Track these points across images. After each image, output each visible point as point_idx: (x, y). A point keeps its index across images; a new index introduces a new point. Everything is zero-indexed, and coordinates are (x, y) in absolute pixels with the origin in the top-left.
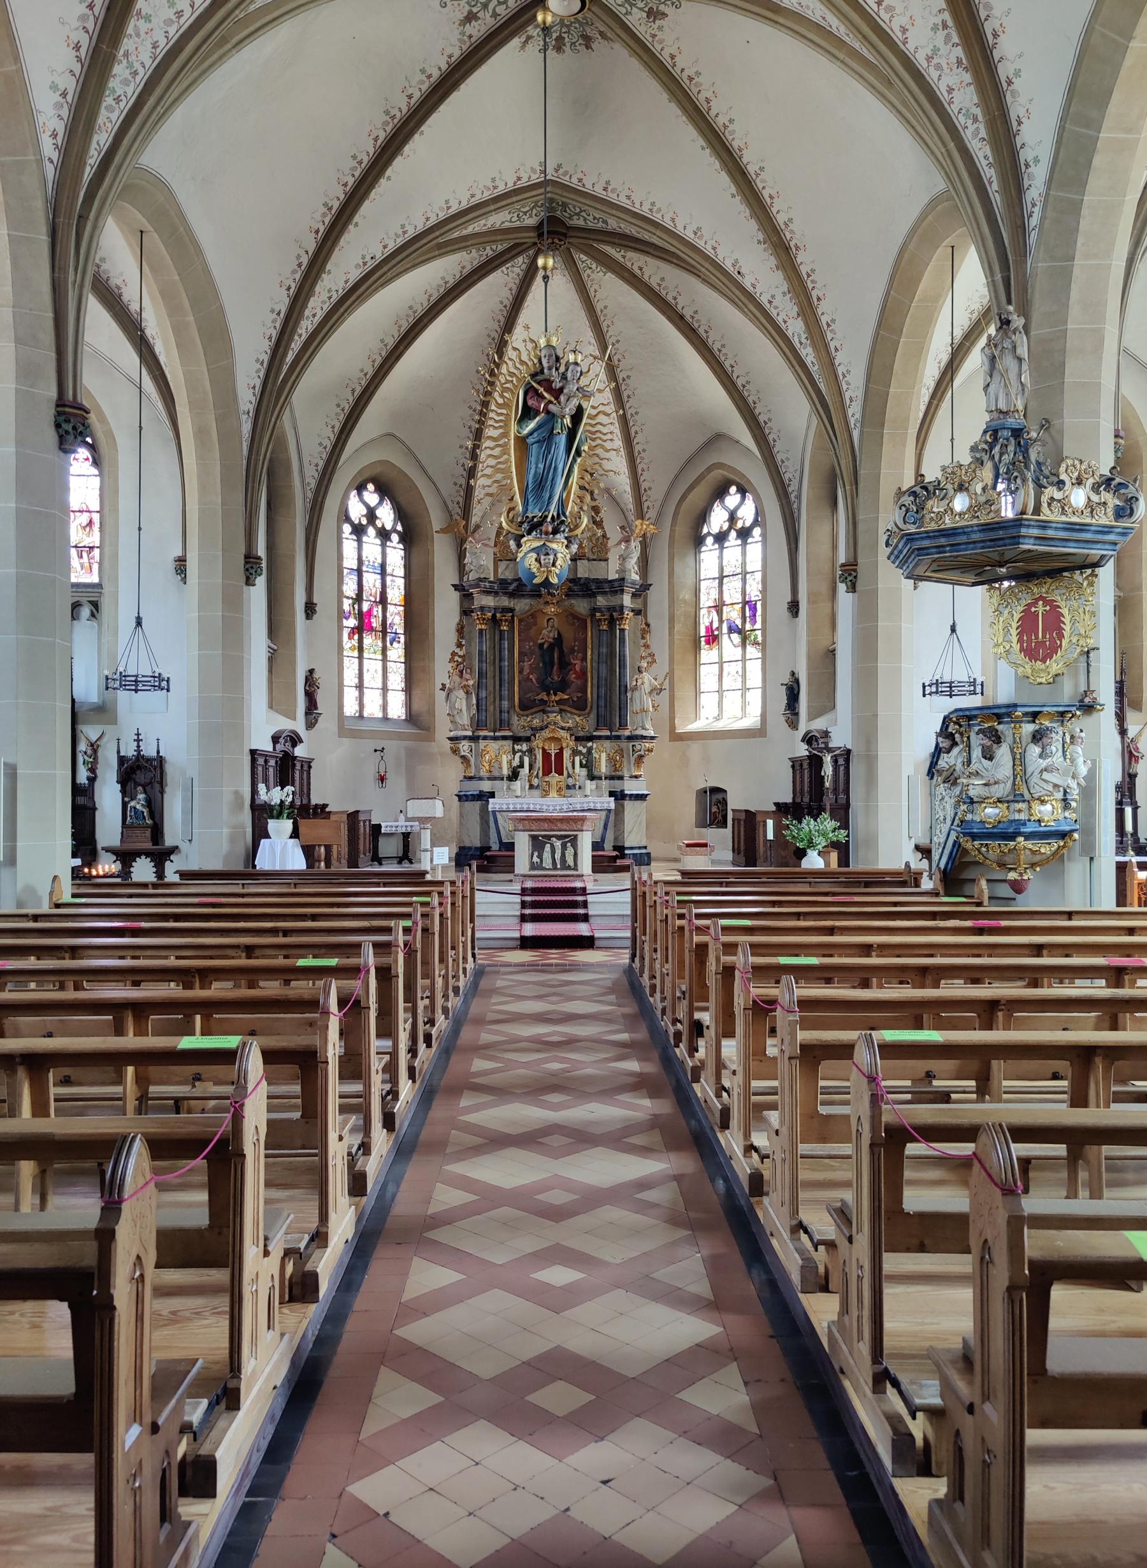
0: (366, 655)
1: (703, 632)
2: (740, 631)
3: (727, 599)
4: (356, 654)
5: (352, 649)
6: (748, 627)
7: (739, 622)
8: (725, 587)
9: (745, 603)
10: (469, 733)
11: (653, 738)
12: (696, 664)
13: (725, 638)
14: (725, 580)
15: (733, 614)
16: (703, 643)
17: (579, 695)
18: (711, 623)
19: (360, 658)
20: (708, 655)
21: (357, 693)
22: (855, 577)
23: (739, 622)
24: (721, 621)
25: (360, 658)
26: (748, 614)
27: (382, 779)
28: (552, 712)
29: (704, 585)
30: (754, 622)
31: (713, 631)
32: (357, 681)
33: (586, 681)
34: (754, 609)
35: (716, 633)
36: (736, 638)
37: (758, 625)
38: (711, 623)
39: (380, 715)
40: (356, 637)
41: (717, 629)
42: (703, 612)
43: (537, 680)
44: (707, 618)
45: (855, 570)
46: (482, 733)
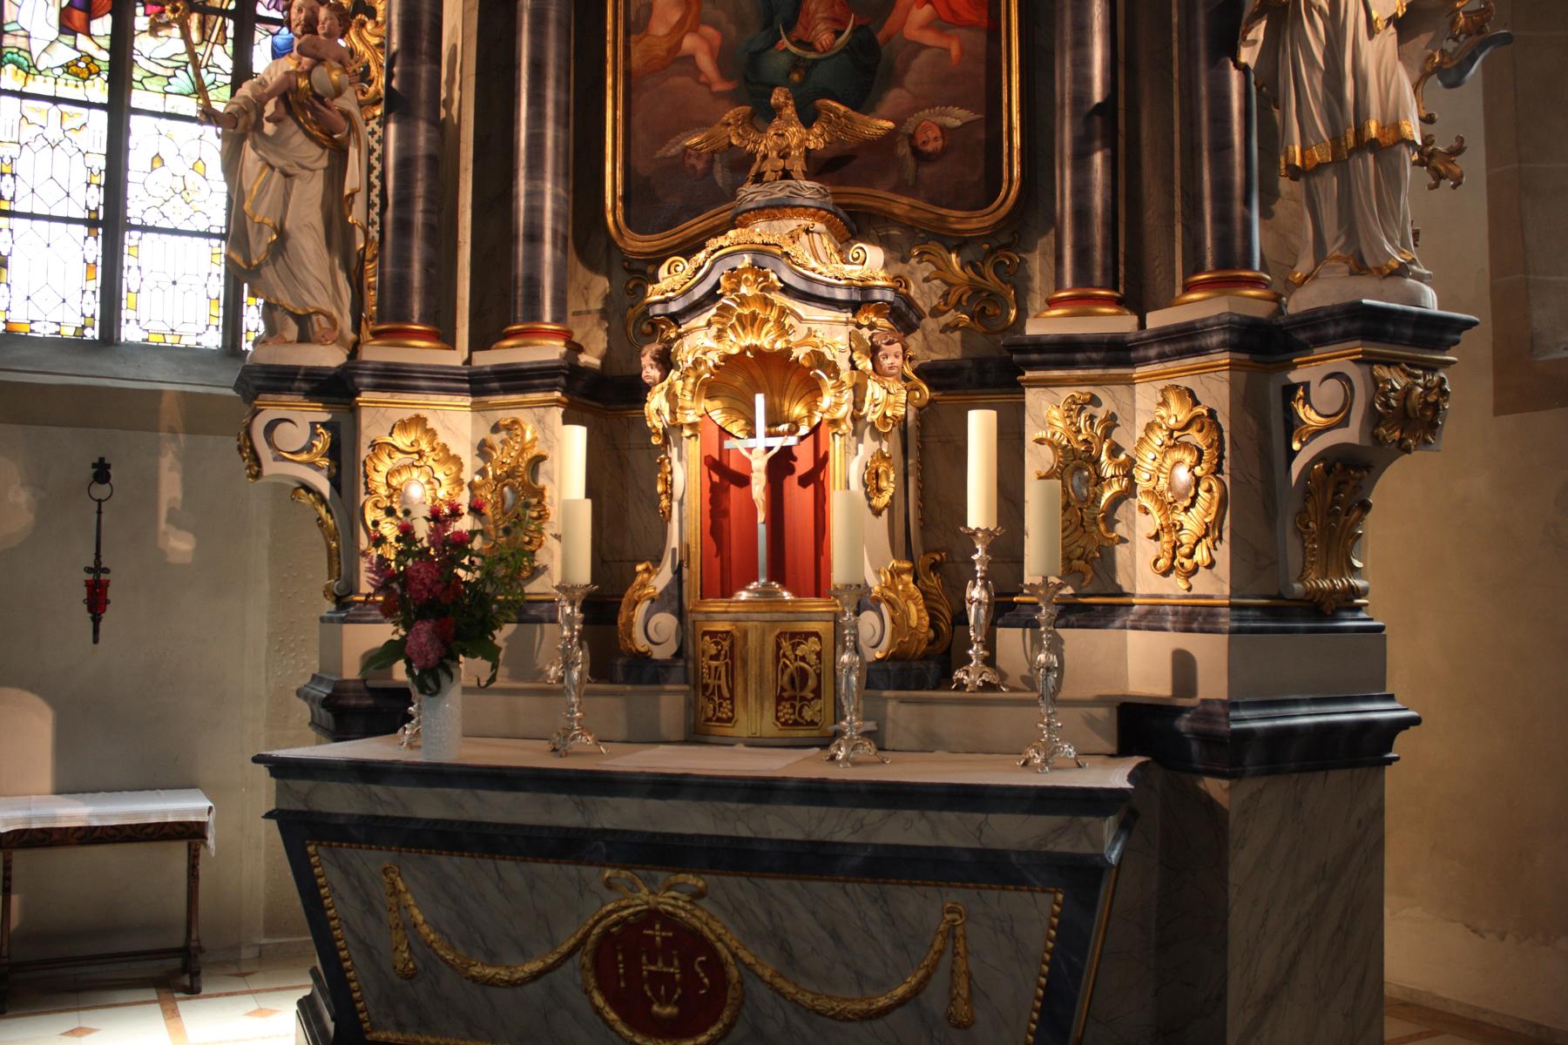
0: (138, 99)
4: (98, 90)
5: (80, 69)
10: (330, 357)
17: (956, 117)
19: (118, 110)
21: (94, 249)
25: (118, 110)
27: (97, 598)
28: (774, 210)
32: (96, 198)
33: (994, 32)
39: (213, 340)
40: (103, 26)
43: (723, 60)
46: (376, 353)
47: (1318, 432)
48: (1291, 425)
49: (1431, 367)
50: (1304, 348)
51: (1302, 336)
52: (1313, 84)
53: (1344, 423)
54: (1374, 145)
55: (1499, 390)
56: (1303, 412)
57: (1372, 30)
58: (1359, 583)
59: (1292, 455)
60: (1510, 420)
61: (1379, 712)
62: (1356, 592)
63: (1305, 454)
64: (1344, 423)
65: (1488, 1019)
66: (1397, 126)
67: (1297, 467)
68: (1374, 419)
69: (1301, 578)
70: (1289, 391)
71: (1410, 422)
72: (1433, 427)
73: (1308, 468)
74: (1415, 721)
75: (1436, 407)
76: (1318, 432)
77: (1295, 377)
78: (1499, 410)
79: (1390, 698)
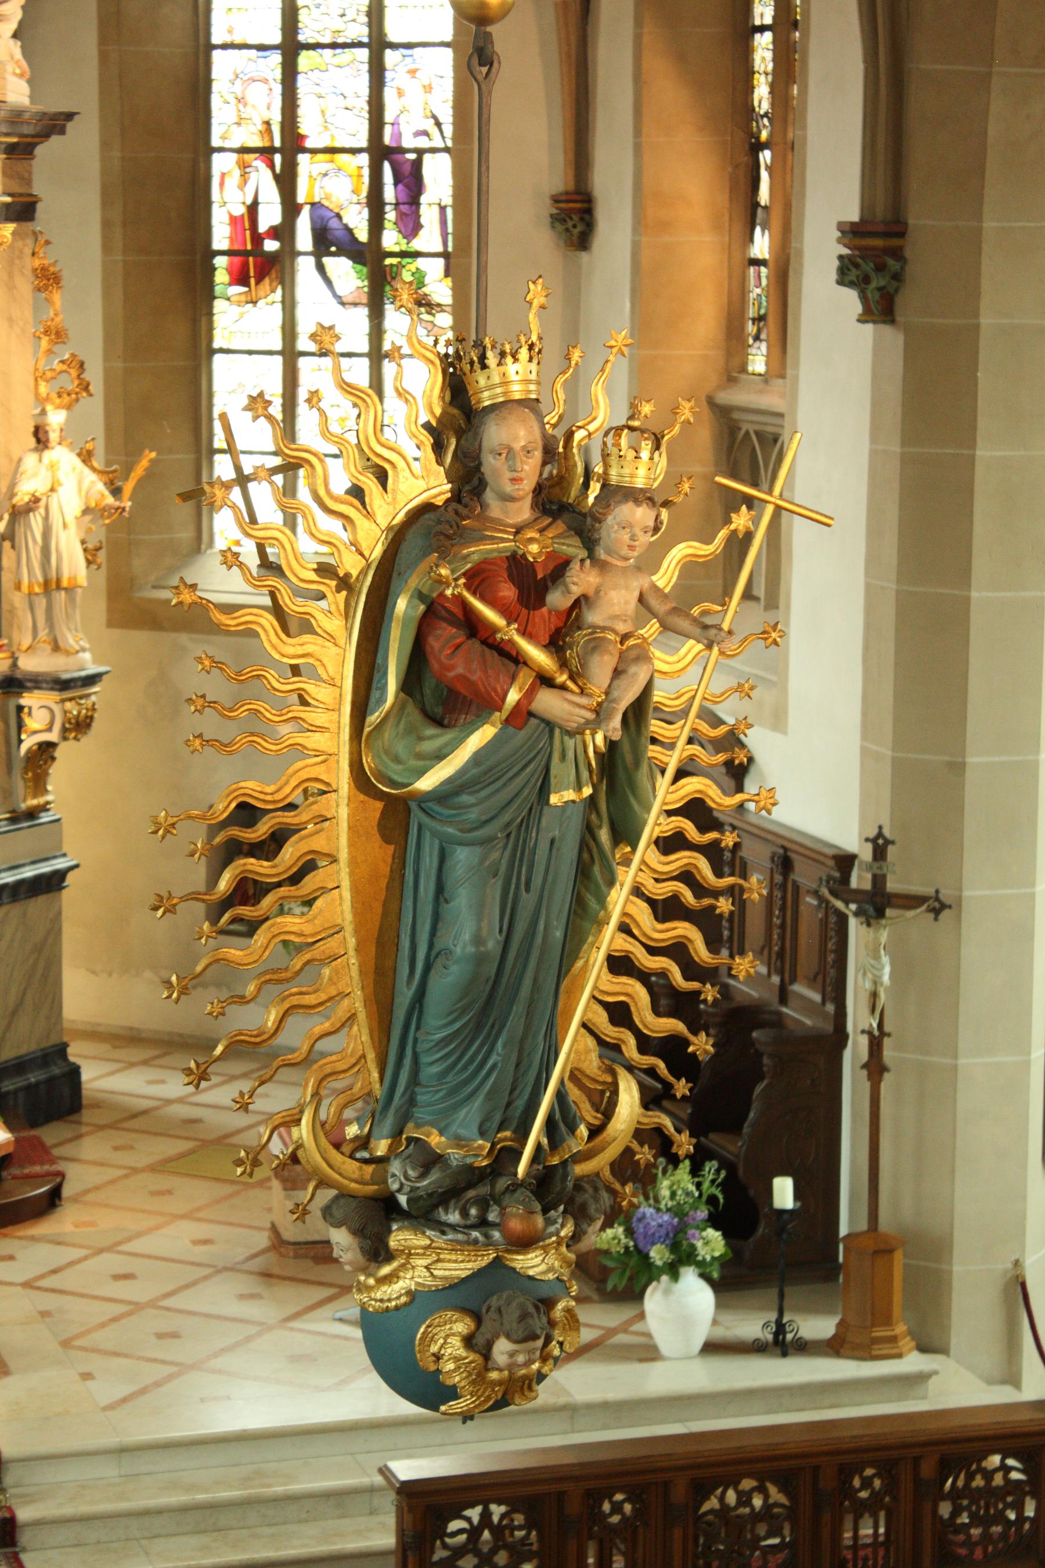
1: (221, 237)
2: (369, 256)
3: (311, 127)
6: (391, 239)
7: (358, 222)
8: (302, 83)
9: (380, 152)
11: (91, 680)
12: (199, 350)
13: (305, 266)
14: (305, 60)
15: (336, 186)
16: (221, 277)
18: (253, 209)
20: (242, 321)
22: (897, 277)
23: (358, 222)
24: (291, 208)
26: (389, 193)
29: (223, 66)
30: (411, 226)
31: (258, 239)
34: (412, 182)
35: (271, 245)
36: (345, 272)
37: (430, 238)
38: (253, 209)
41: (274, 233)
42: (220, 163)
44: (239, 190)
45: (897, 254)
47: (35, 732)
48: (20, 726)
49: (88, 696)
50: (29, 689)
51: (29, 684)
52: (36, 553)
53: (49, 729)
54: (65, 589)
55: (110, 610)
56: (27, 720)
57: (65, 526)
58: (50, 798)
59: (20, 741)
60: (117, 633)
61: (60, 864)
62: (48, 803)
63: (29, 743)
64: (49, 729)
65: (101, 1029)
66: (75, 578)
67: (24, 748)
68: (64, 730)
69: (24, 800)
70: (20, 708)
71: (80, 726)
72: (89, 726)
73: (29, 751)
74: (77, 866)
75: (92, 718)
76: (35, 732)
77: (23, 702)
78: (111, 624)
79: (64, 855)
